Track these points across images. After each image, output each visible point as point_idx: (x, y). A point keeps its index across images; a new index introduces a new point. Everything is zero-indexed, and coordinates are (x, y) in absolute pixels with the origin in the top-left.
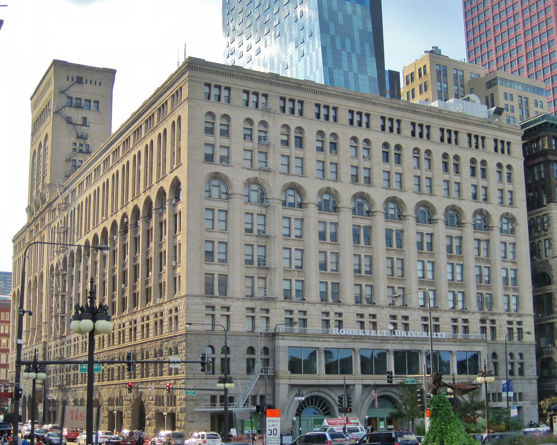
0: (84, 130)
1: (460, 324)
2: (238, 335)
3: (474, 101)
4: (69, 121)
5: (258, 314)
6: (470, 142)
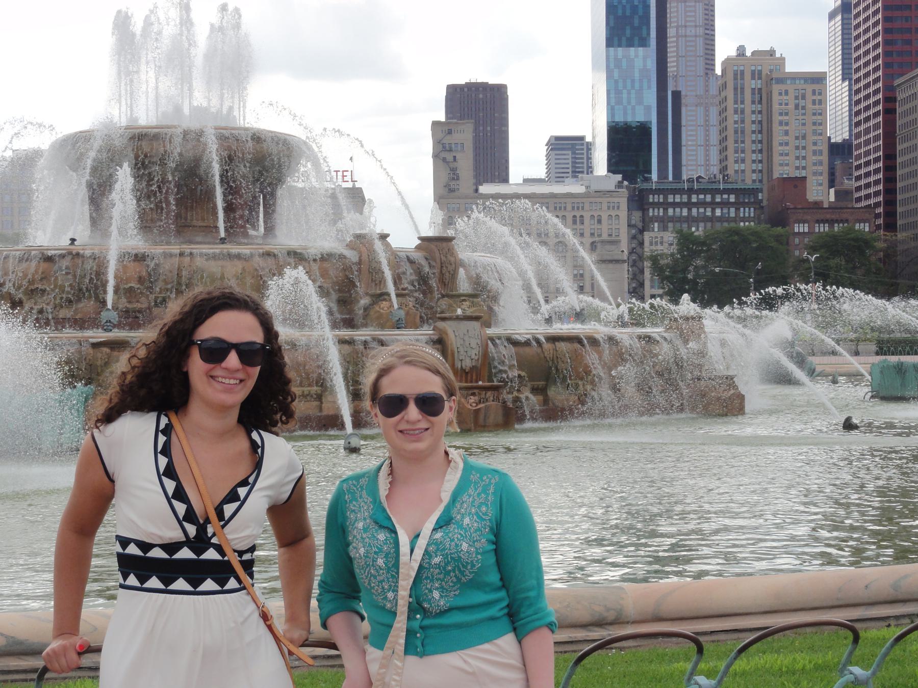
4: (444, 160)
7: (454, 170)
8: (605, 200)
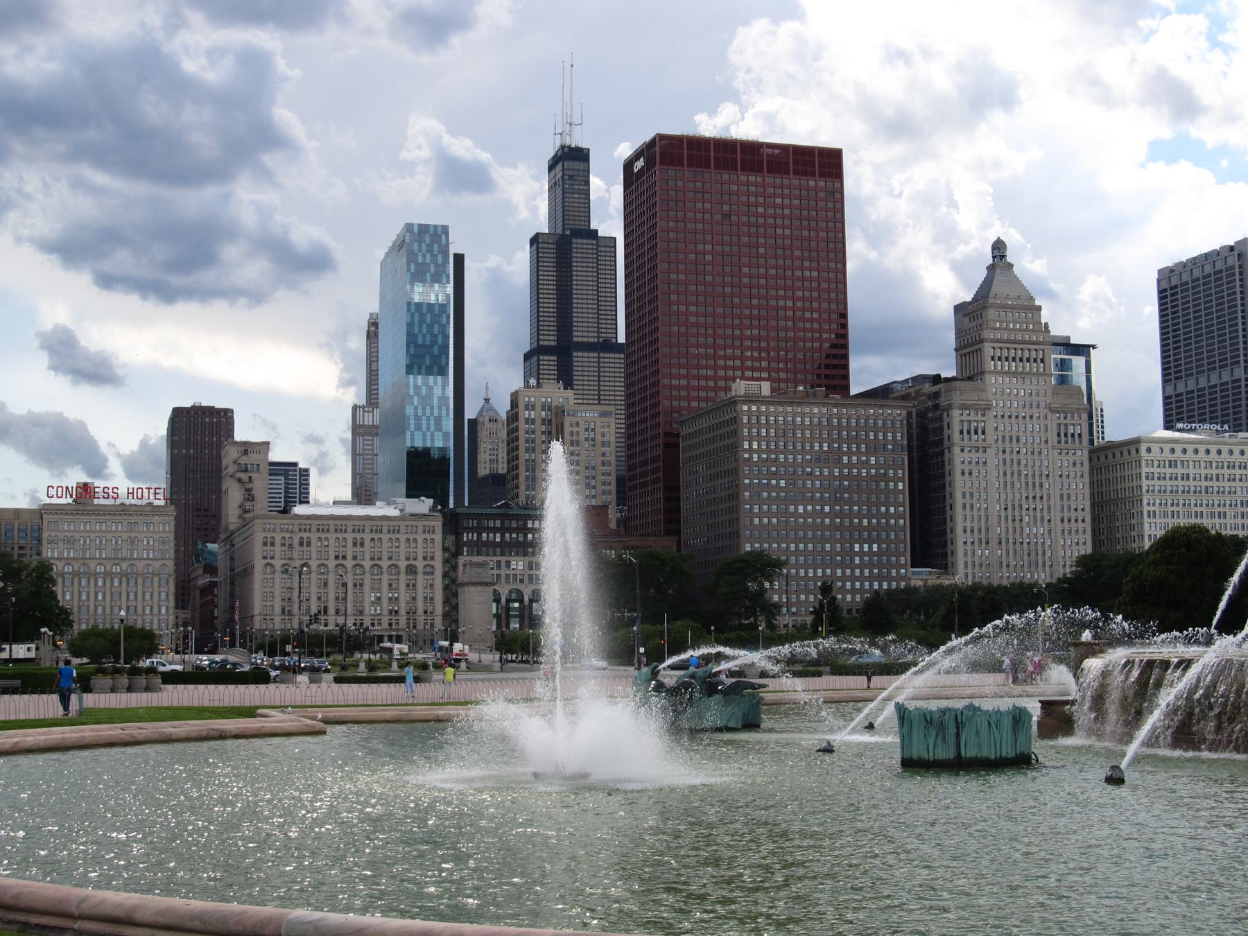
0: (250, 485)
4: (240, 480)
7: (249, 490)
8: (420, 524)
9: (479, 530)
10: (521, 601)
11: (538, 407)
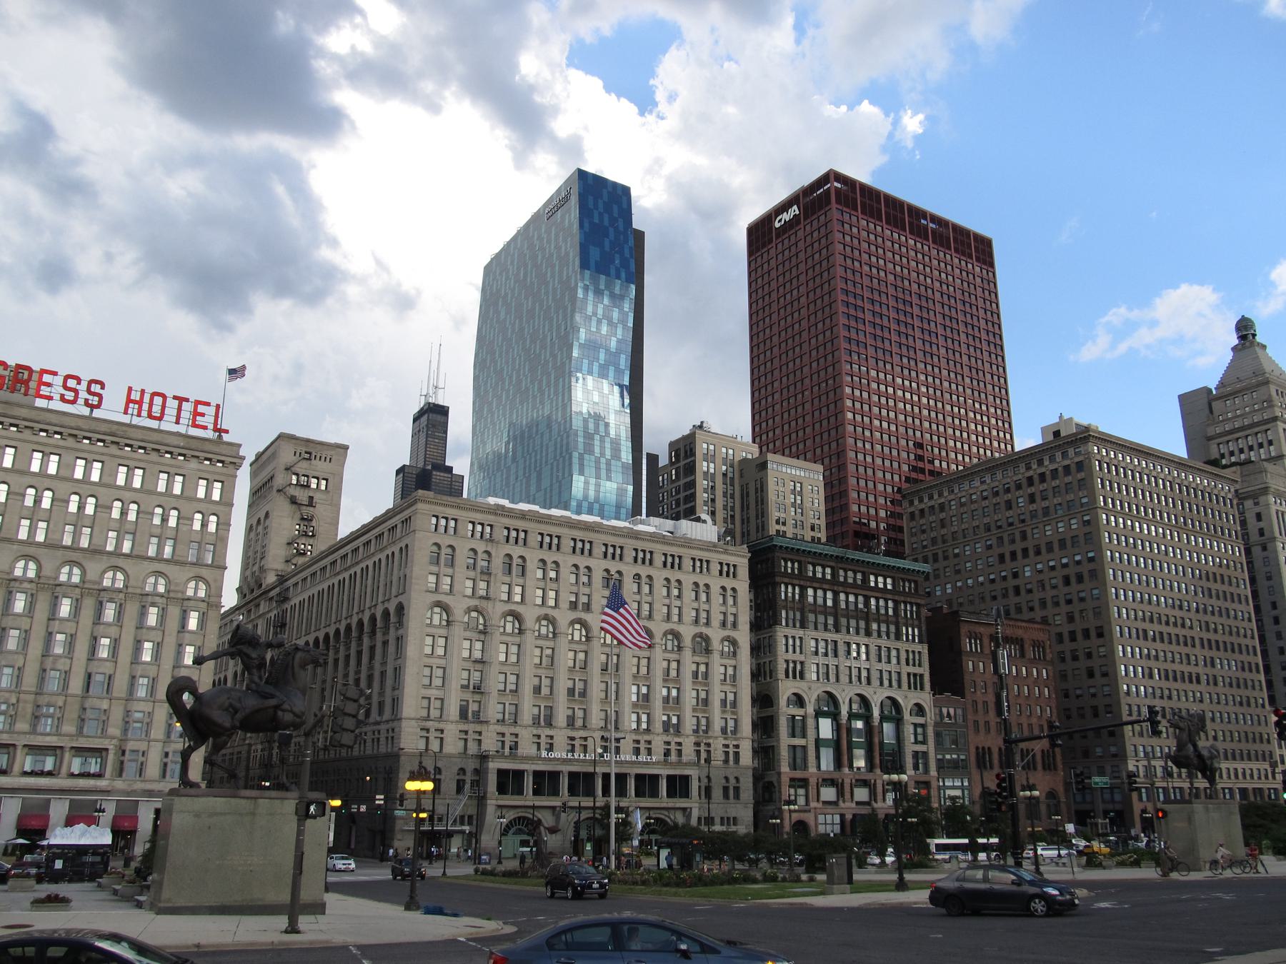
1: (673, 747)
2: (450, 756)
3: (704, 522)
4: (293, 501)
5: (471, 736)
6: (694, 566)
7: (307, 520)
9: (804, 581)
10: (867, 719)
11: (719, 461)
